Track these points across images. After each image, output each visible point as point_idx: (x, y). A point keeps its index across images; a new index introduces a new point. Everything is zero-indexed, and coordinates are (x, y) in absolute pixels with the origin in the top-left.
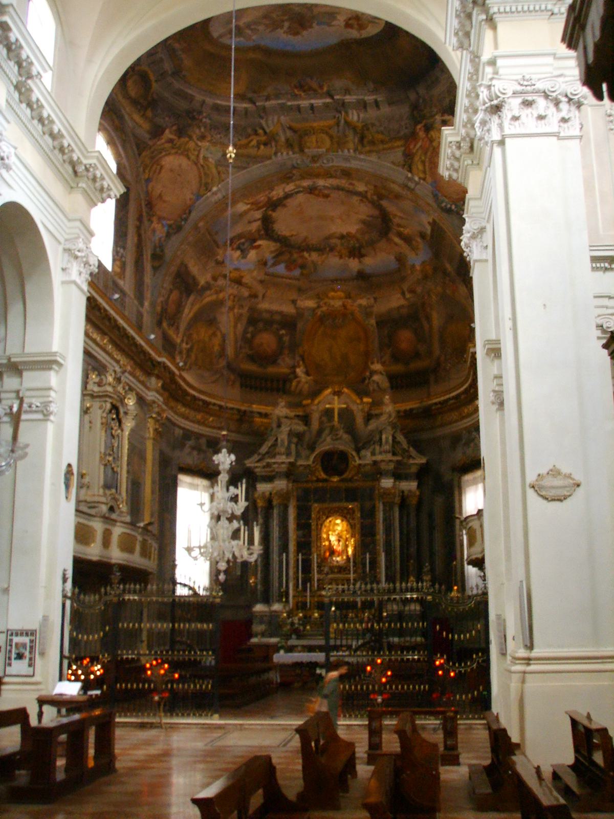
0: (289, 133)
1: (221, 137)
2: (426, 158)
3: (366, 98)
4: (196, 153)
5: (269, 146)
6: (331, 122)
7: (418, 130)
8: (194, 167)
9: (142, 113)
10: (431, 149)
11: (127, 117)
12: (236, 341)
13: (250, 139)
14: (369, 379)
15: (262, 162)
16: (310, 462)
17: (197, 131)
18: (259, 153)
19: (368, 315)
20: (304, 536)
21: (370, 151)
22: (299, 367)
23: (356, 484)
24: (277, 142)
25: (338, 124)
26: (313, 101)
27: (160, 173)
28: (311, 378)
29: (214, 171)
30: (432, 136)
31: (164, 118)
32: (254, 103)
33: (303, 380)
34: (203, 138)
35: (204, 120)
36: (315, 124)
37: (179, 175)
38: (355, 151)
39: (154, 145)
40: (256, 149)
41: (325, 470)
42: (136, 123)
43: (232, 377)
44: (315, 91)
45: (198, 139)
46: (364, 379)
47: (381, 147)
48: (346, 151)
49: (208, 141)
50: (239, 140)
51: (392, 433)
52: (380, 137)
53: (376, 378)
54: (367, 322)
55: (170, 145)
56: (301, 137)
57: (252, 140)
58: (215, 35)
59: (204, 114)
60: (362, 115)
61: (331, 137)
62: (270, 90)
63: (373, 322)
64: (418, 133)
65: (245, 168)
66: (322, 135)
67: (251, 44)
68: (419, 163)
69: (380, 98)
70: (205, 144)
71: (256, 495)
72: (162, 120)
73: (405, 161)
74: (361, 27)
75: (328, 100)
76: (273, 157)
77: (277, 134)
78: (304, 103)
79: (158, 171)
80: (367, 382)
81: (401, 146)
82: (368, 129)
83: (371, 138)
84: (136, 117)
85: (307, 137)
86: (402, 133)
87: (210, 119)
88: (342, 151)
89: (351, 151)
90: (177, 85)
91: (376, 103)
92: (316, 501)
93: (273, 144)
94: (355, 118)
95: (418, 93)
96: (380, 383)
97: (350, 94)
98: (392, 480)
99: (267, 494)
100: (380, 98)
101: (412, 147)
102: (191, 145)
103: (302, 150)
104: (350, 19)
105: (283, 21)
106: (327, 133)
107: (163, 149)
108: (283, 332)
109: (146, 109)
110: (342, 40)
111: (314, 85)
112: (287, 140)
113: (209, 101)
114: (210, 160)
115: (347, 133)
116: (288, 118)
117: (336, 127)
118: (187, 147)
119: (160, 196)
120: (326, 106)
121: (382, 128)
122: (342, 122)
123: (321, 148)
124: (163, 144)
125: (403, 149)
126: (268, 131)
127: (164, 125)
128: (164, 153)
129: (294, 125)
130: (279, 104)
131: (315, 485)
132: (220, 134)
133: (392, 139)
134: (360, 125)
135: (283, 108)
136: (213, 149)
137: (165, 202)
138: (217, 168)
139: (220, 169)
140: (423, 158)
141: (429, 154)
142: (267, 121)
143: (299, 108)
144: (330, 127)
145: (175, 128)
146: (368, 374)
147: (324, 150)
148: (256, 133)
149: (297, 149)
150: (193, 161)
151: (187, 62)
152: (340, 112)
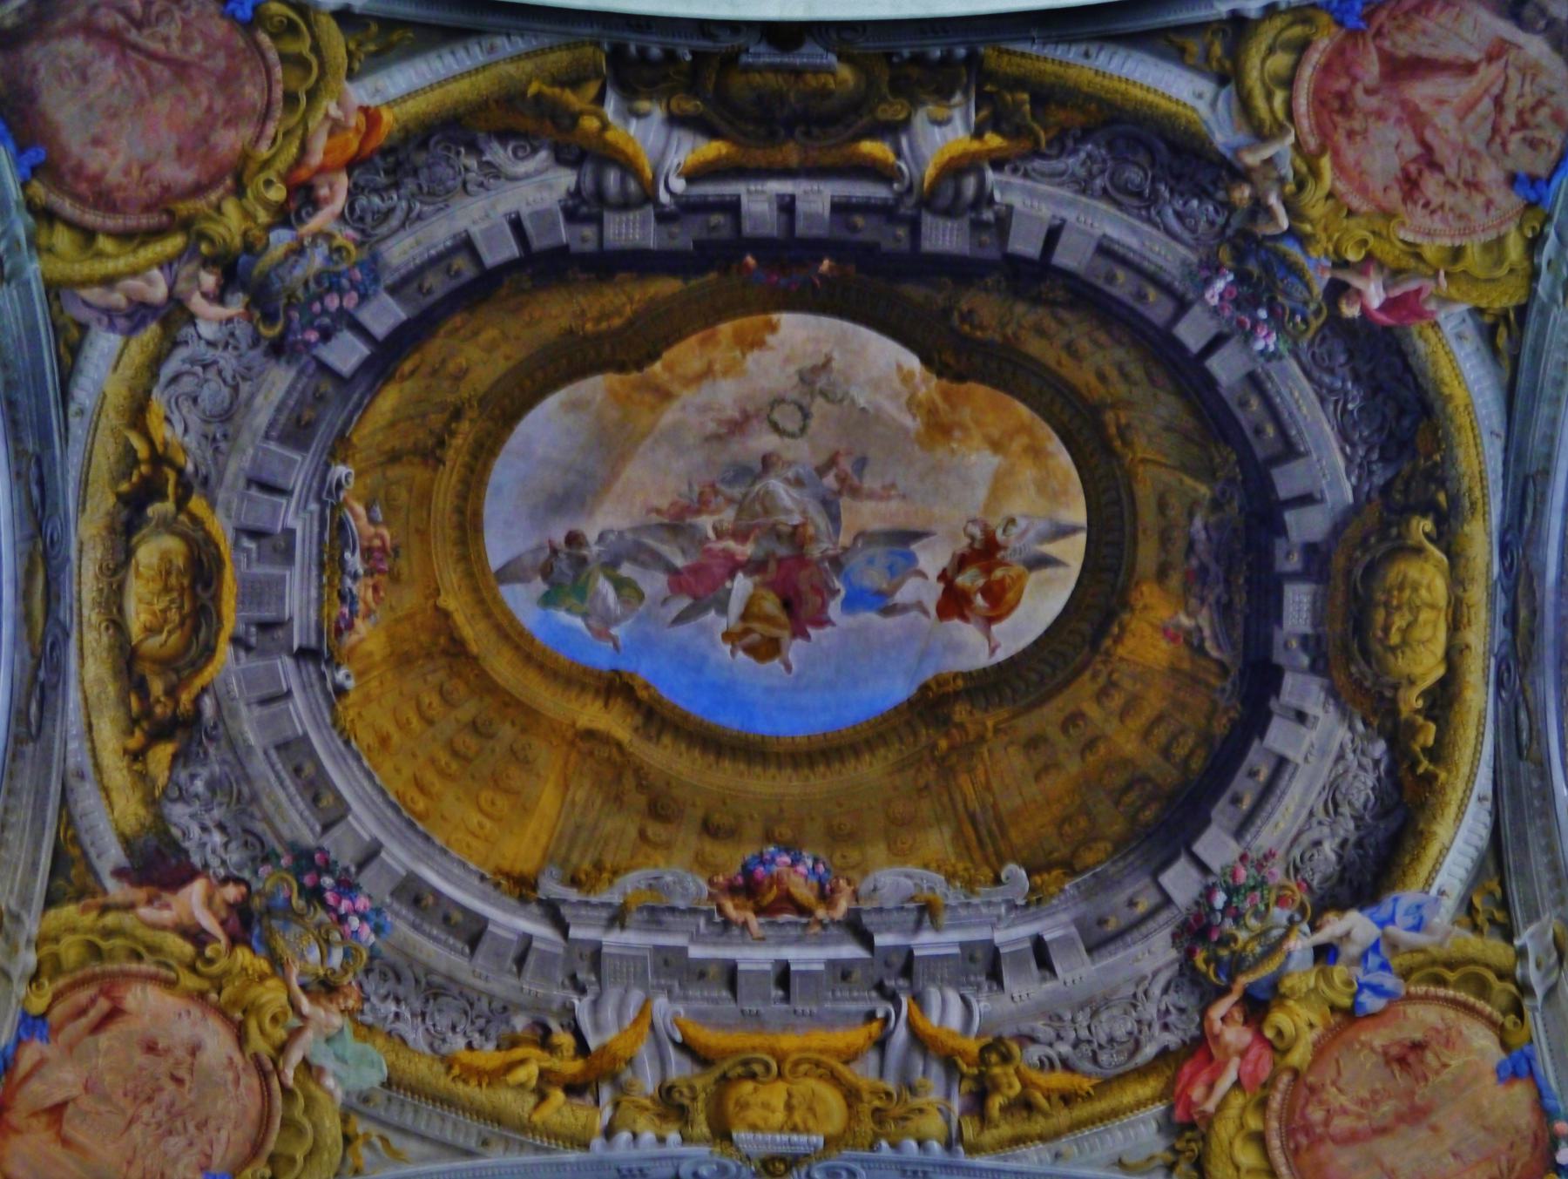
0: (679, 1068)
1: (397, 1015)
2: (1265, 1121)
3: (999, 937)
4: (280, 1034)
5: (589, 1098)
6: (858, 1036)
7: (1218, 1025)
8: (255, 1082)
9: (134, 742)
10: (1285, 1078)
11: (74, 696)
13: (518, 1053)
15: (548, 1151)
17: (314, 955)
18: (536, 1118)
21: (1018, 1140)
24: (621, 1089)
25: (881, 1044)
26: (790, 953)
27: (98, 1027)
29: (332, 1127)
30: (1280, 1033)
31: (204, 829)
32: (562, 927)
34: (326, 988)
35: (354, 922)
36: (789, 1042)
37: (179, 1081)
38: (948, 1146)
39: (130, 907)
40: (531, 1100)
42: (97, 766)
44: (803, 910)
45: (303, 987)
47: (1063, 1117)
48: (913, 1144)
49: (345, 1012)
50: (470, 1046)
52: (1059, 1079)
55: (188, 949)
56: (725, 1080)
57: (522, 1062)
58: (497, 555)
59: (362, 903)
60: (980, 1006)
61: (851, 1096)
62: (630, 884)
64: (1217, 1038)
65: (469, 1153)
66: (812, 1083)
67: (601, 658)
68: (1238, 1144)
69: (1054, 927)
70: (326, 1016)
72: (195, 831)
73: (1172, 1149)
74: (1000, 601)
75: (850, 951)
76: (597, 1143)
77: (630, 1062)
78: (756, 957)
79: (94, 1015)
81: (1153, 1100)
82: (1006, 1058)
83: (1018, 1087)
84: (108, 734)
85: (748, 1086)
86: (1149, 1051)
87: (378, 930)
88: (894, 1146)
89: (936, 1146)
90: (301, 713)
91: (1041, 953)
93: (606, 1093)
94: (955, 1019)
95: (1204, 868)
97: (936, 928)
100: (1054, 927)
101: (1197, 1093)
102: (272, 995)
103: (722, 1133)
104: (962, 562)
105: (734, 567)
106: (834, 1079)
107: (153, 949)
109: (159, 733)
110: (925, 688)
111: (803, 890)
112: (666, 1092)
113: (398, 856)
114: (330, 1082)
115: (918, 1077)
116: (680, 1008)
117: (873, 1058)
118: (255, 992)
119: (56, 1112)
120: (842, 972)
121: (1064, 1049)
122: (901, 1035)
123: (808, 1131)
124: (163, 928)
125: (1160, 1107)
126: (593, 1043)
127: (196, 860)
128: (148, 966)
129: (708, 1037)
130: (658, 949)
132: (398, 1001)
133: (1107, 1084)
134: (972, 1046)
135: (673, 966)
136: (351, 1045)
137: (66, 1142)
138: (345, 1120)
139: (360, 1127)
140: (1254, 1123)
141: (1276, 1102)
142: (596, 1005)
143: (731, 975)
144: (850, 1057)
145: (232, 892)
147: (818, 1140)
148: (544, 1039)
149: (702, 1128)
150: (256, 1058)
151: (367, 636)
152: (893, 998)
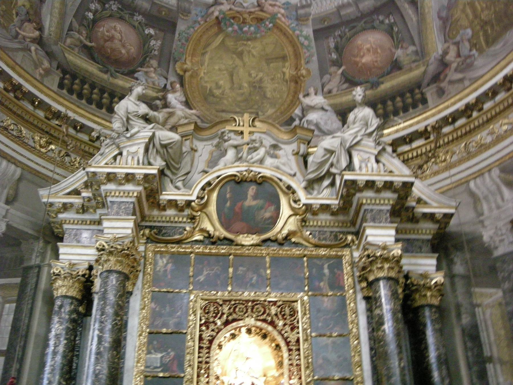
12: (63, 15)
14: (301, 120)
16: (194, 198)
19: (301, 19)
20: (165, 367)
22: (174, 91)
23: (296, 251)
28: (194, 111)
33: (179, 113)
41: (226, 225)
43: (46, 64)
46: (292, 120)
51: (376, 152)
53: (313, 116)
54: (297, 32)
63: (308, 31)
71: (57, 267)
80: (297, 122)
92: (200, 286)
96: (322, 123)
98: (393, 232)
99: (82, 269)
108: (152, 31)
131: (200, 249)
146: (298, 111)
